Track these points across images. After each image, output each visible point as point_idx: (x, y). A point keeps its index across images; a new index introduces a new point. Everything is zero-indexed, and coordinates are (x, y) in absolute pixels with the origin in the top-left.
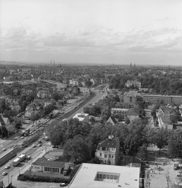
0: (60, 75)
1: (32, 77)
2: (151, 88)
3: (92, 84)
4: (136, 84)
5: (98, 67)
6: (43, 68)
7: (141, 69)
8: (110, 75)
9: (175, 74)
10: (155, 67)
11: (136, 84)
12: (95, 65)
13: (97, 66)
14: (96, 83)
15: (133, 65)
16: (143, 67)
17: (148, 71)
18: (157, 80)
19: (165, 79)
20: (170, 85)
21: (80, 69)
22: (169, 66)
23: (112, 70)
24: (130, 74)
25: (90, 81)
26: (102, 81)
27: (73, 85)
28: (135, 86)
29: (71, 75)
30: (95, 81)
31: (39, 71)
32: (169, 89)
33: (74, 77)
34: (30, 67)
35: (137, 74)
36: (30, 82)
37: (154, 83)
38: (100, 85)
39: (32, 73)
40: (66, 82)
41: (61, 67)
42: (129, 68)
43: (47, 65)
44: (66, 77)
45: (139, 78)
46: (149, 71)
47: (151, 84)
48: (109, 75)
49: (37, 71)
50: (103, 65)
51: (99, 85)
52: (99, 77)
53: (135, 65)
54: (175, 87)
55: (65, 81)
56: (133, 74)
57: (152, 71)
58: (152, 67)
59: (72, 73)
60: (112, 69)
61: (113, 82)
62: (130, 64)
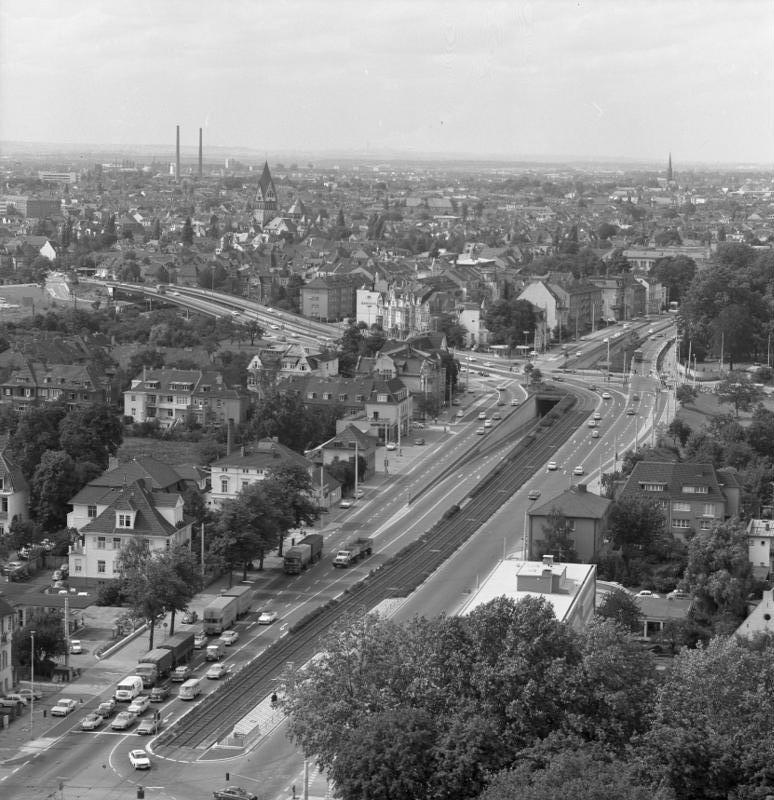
0: (263, 247)
1: (47, 265)
3: (539, 325)
5: (553, 189)
6: (116, 187)
8: (671, 252)
12: (517, 173)
13: (537, 184)
14: (571, 320)
21: (412, 202)
23: (672, 213)
25: (521, 298)
26: (610, 298)
27: (388, 327)
29: (361, 254)
30: (556, 297)
31: (90, 216)
33: (390, 266)
34: (14, 183)
36: (36, 300)
38: (595, 334)
39: (43, 231)
40: (330, 305)
41: (269, 189)
43: (146, 169)
44: (322, 267)
48: (657, 255)
49: (74, 212)
51: (588, 330)
52: (589, 271)
55: (324, 298)
59: (357, 232)
60: (666, 207)
61: (707, 307)
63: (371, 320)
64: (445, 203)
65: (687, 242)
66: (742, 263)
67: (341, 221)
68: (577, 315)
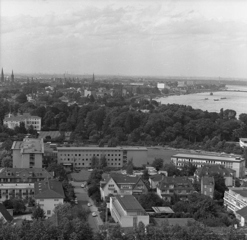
2: (66, 131)
4: (28, 123)
7: (28, 84)
9: (112, 94)
10: (60, 80)
11: (28, 123)
15: (7, 75)
16: (32, 80)
17: (47, 90)
18: (78, 112)
19: (96, 108)
20: (112, 123)
22: (92, 77)
24: (6, 96)
28: (27, 127)
32: (109, 132)
35: (23, 99)
37: (71, 119)
45: (31, 106)
46: (49, 90)
47: (65, 121)
53: (13, 76)
54: (123, 126)
56: (14, 97)
57: (55, 89)
58: (52, 79)
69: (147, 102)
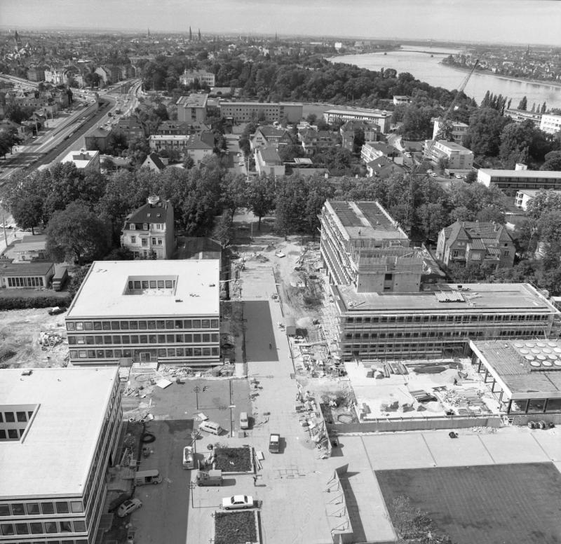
0: (18, 58)
3: (101, 81)
4: (203, 79)
5: (114, 39)
7: (214, 42)
8: (143, 58)
10: (245, 38)
11: (203, 79)
12: (103, 33)
13: (108, 37)
14: (111, 79)
19: (267, 66)
20: (278, 80)
23: (148, 46)
24: (190, 54)
26: (124, 72)
27: (55, 82)
28: (201, 82)
29: (48, 60)
32: (275, 89)
33: (56, 63)
35: (205, 56)
37: (243, 76)
42: (187, 40)
44: (35, 64)
45: (209, 63)
46: (232, 48)
47: (237, 78)
48: (139, 58)
50: (123, 32)
51: (117, 81)
52: (118, 64)
53: (200, 34)
56: (197, 55)
57: (238, 47)
58: (239, 37)
60: (146, 44)
61: (150, 74)
62: (188, 31)
63: (50, 80)
64: (78, 43)
65: (150, 55)
66: (162, 61)
67: (44, 50)
68: (113, 77)
69: (319, 61)
